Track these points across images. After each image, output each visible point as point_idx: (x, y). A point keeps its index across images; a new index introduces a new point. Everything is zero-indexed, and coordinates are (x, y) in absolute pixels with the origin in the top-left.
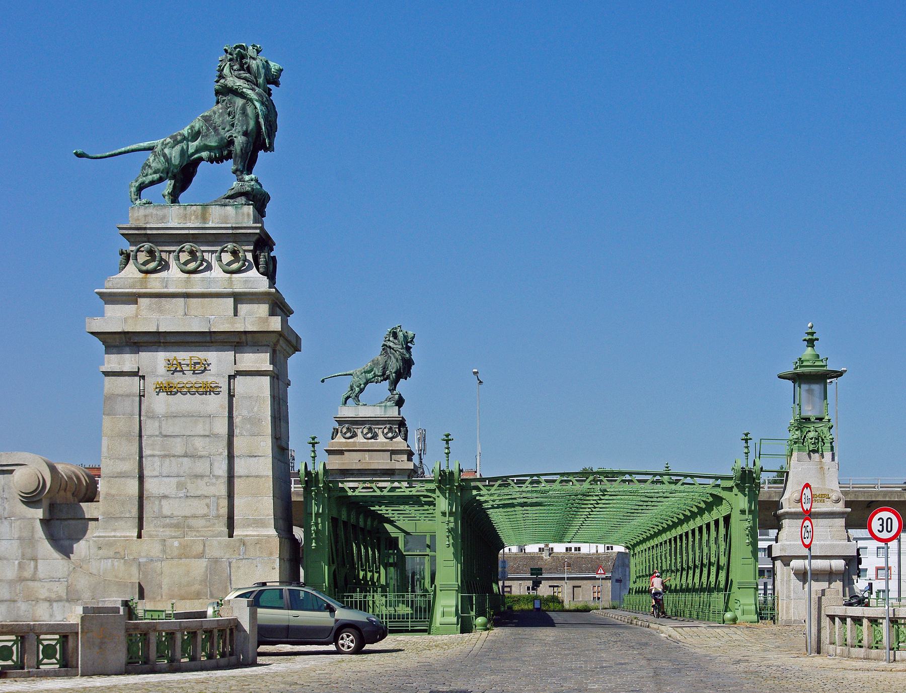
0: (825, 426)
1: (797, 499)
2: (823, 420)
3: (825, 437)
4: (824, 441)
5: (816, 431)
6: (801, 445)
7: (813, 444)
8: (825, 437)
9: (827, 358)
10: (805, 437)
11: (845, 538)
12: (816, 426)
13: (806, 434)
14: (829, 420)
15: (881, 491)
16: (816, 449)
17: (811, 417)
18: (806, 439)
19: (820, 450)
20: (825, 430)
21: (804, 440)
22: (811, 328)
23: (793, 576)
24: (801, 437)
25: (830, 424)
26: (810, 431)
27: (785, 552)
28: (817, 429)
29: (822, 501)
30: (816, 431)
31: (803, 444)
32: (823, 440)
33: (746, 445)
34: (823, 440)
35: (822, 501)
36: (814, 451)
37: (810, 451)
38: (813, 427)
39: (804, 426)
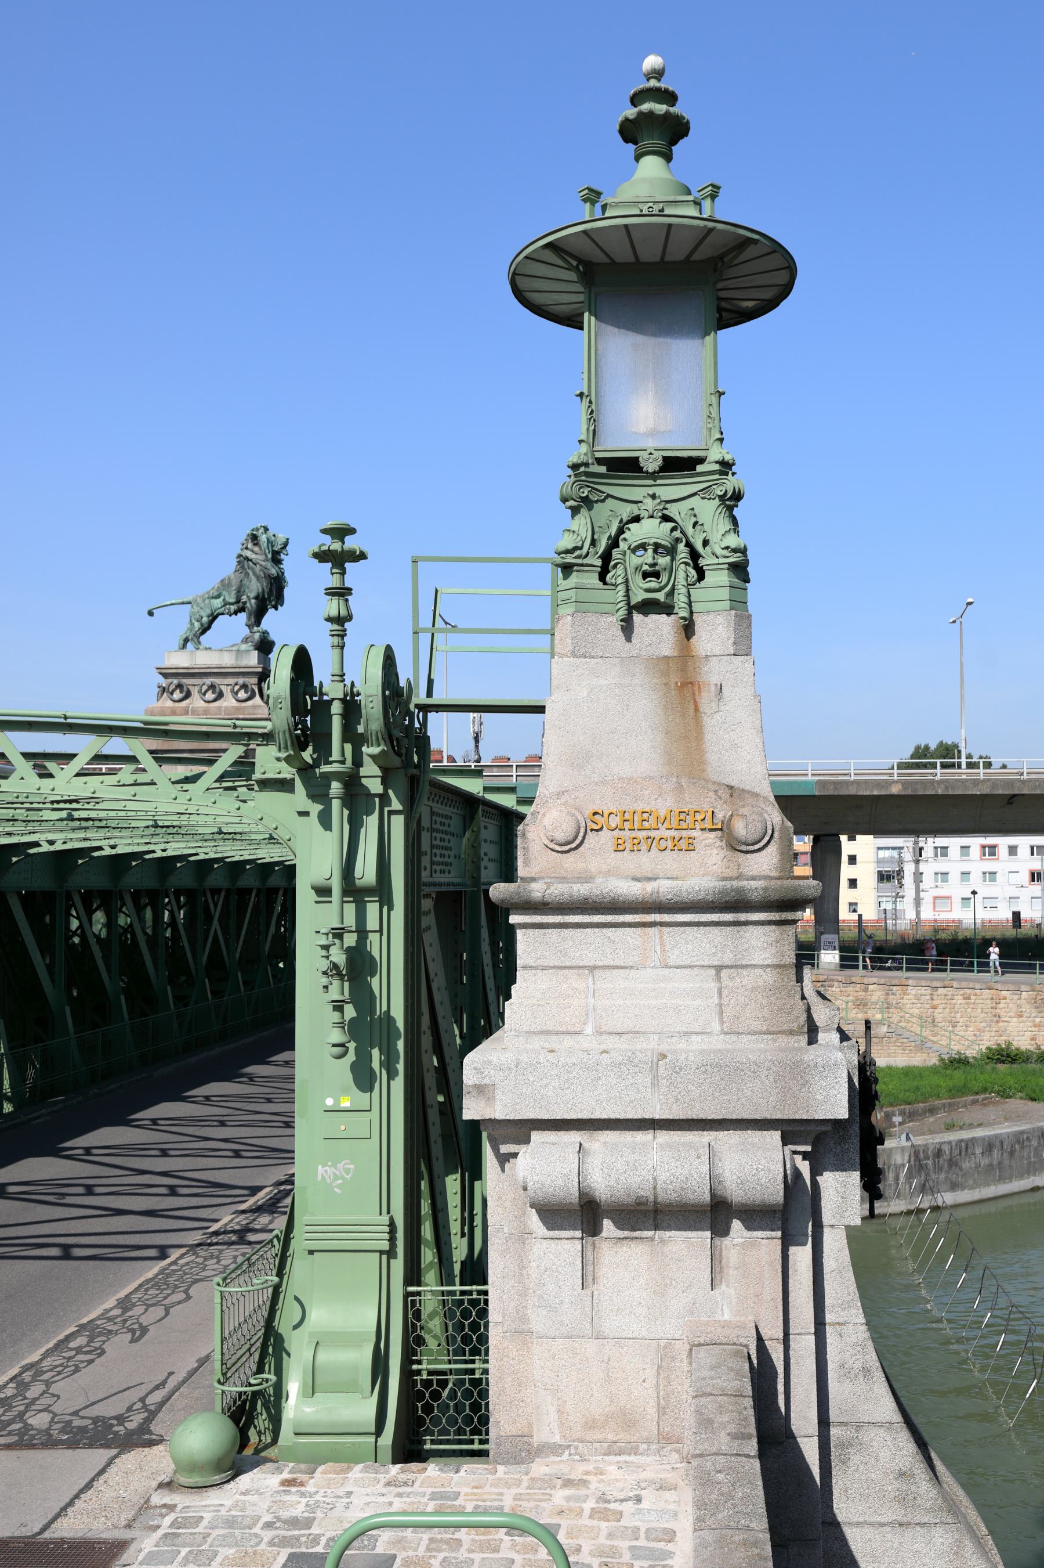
0: (705, 493)
1: (561, 836)
2: (700, 468)
3: (706, 543)
4: (702, 562)
5: (666, 518)
6: (594, 579)
7: (646, 575)
8: (706, 543)
9: (716, 188)
10: (614, 543)
11: (795, 1026)
12: (667, 492)
13: (621, 531)
14: (726, 467)
15: (1030, 780)
16: (661, 596)
17: (643, 456)
18: (615, 553)
19: (680, 599)
20: (708, 510)
21: (606, 557)
22: (658, 74)
23: (534, 1220)
24: (593, 543)
25: (730, 484)
26: (637, 519)
27: (490, 1099)
28: (673, 511)
29: (683, 844)
30: (666, 518)
31: (602, 578)
32: (695, 555)
33: (334, 581)
34: (695, 555)
35: (683, 844)
36: (648, 607)
37: (631, 609)
38: (653, 497)
39: (609, 496)
